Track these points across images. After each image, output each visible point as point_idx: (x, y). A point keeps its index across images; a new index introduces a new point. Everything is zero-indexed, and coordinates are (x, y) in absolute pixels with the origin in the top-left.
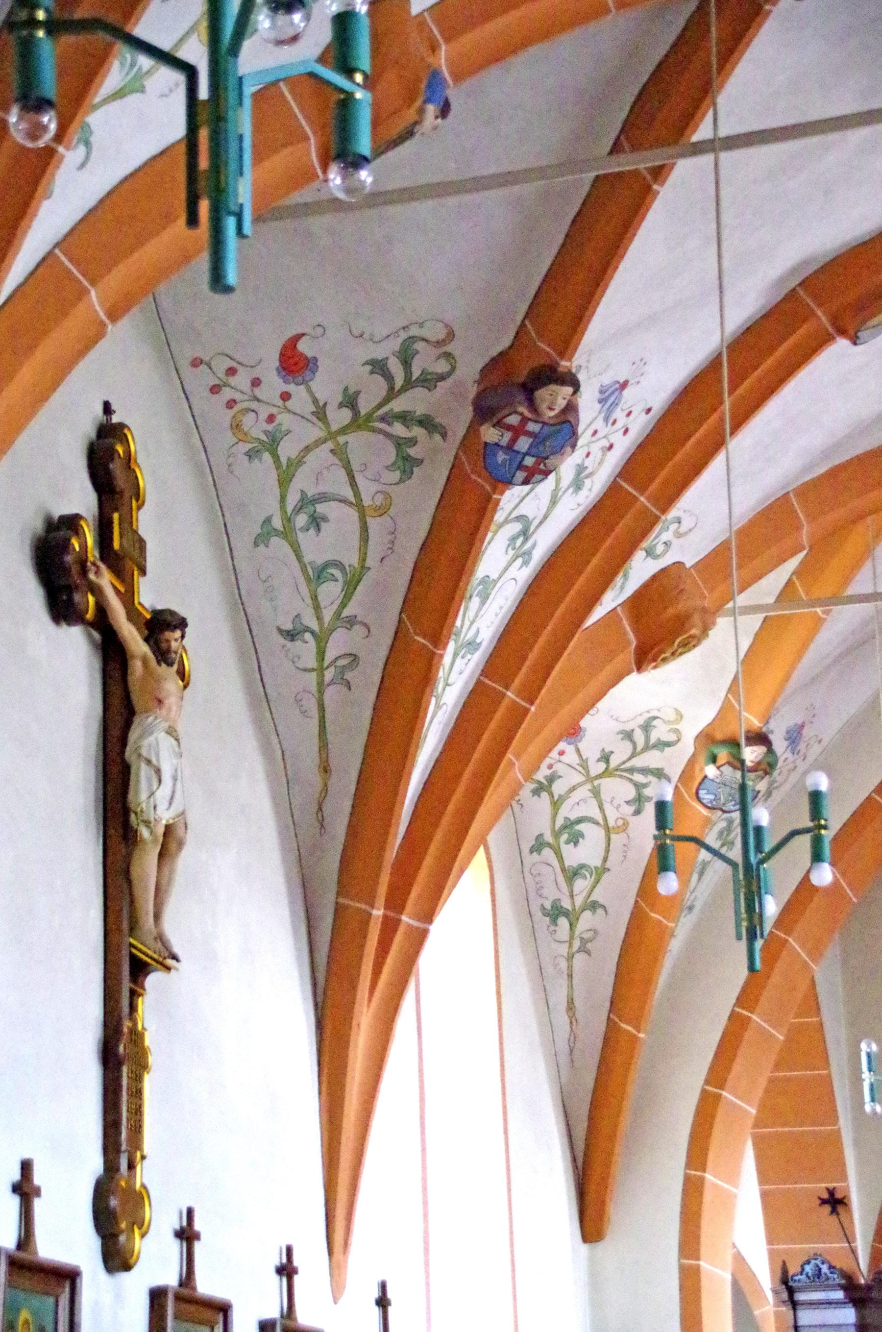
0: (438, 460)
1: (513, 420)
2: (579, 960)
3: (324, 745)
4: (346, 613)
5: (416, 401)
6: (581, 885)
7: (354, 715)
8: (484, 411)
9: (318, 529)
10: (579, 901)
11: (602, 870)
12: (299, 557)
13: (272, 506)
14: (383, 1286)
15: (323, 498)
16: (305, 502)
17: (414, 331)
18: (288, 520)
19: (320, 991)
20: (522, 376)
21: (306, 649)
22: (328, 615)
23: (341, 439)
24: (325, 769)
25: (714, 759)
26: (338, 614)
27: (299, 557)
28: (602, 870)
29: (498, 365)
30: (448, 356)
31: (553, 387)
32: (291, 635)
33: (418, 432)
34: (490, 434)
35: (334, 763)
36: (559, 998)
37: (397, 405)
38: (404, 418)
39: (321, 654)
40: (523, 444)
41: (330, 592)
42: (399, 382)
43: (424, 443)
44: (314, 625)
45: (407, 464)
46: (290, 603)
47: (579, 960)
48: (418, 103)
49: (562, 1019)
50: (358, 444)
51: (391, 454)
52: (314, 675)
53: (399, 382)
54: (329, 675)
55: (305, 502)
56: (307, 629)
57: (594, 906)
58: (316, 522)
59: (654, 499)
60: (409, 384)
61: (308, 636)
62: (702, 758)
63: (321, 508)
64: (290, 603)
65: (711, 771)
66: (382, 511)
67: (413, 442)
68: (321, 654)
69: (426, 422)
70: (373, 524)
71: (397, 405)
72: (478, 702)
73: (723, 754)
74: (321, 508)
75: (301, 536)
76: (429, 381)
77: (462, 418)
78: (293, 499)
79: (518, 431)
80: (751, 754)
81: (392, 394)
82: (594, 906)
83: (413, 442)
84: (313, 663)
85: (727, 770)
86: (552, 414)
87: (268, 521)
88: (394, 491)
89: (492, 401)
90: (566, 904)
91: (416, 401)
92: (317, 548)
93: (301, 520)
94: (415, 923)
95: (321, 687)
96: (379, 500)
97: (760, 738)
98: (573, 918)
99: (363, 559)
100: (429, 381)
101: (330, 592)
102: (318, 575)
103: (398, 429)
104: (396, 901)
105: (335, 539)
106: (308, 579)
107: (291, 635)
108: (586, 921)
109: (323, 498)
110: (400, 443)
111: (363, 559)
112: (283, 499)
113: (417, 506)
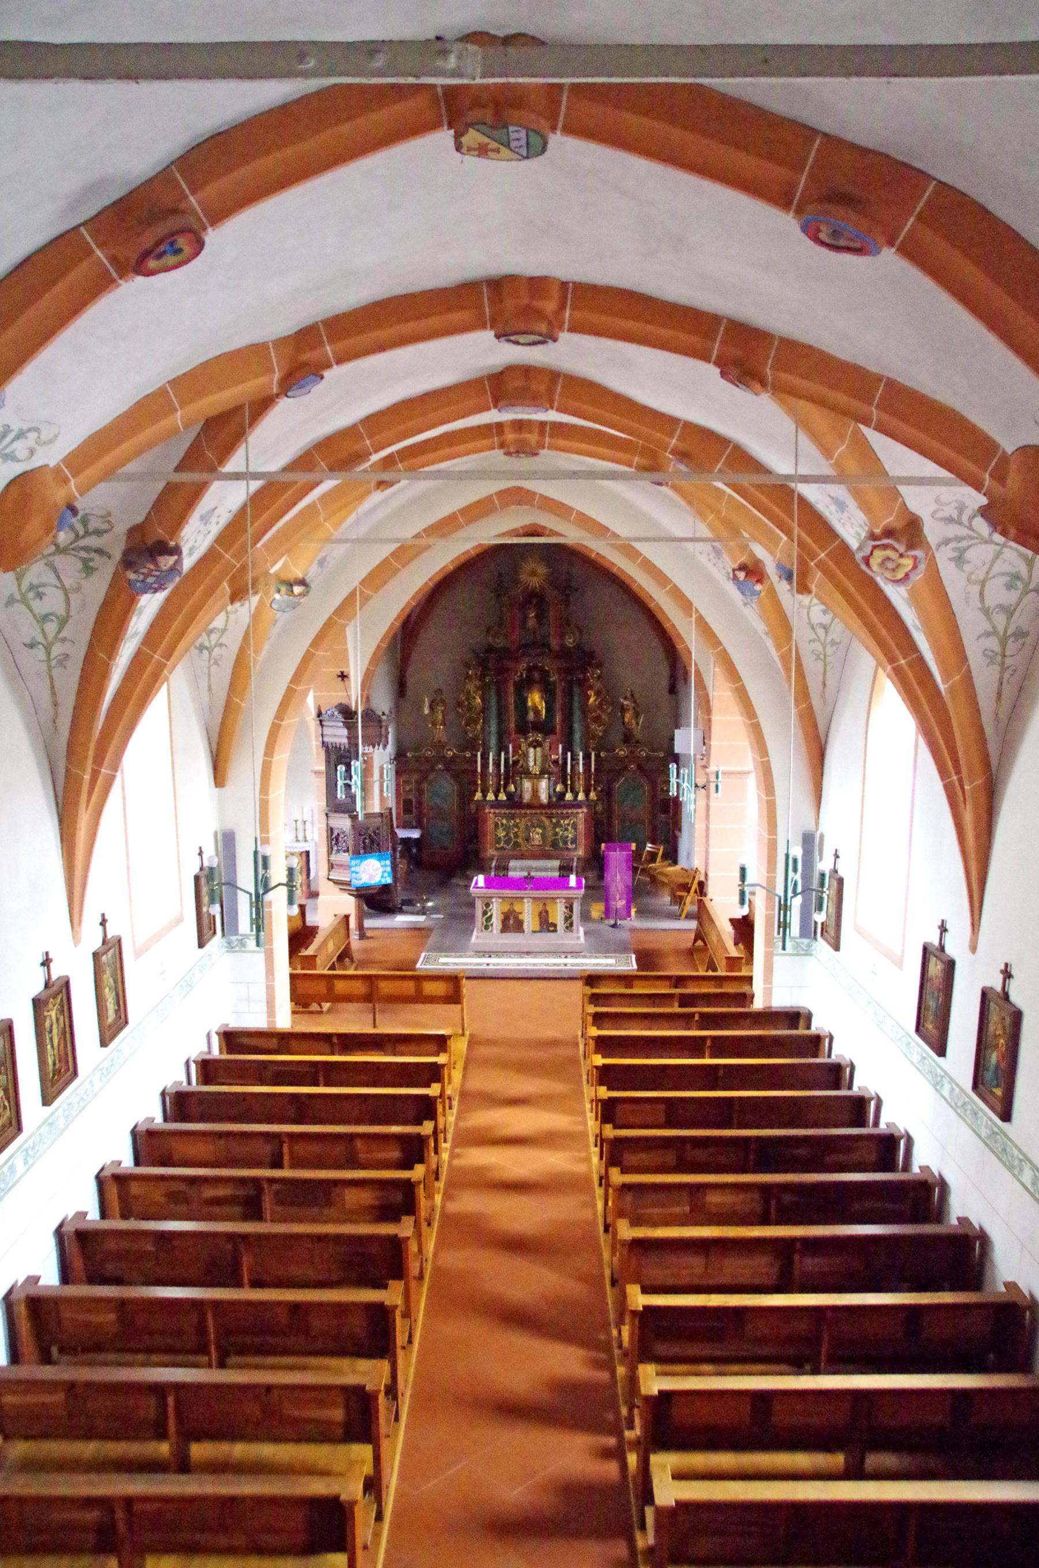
0: (106, 570)
1: (145, 571)
2: (214, 669)
3: (54, 693)
4: (61, 635)
5: (93, 541)
6: (214, 637)
7: (69, 680)
8: (128, 562)
9: (41, 599)
10: (213, 643)
11: (223, 631)
12: (31, 611)
13: (14, 589)
14: (103, 915)
15: (43, 585)
16: (32, 587)
17: (87, 511)
18: (24, 596)
19: (60, 806)
20: (150, 542)
21: (40, 653)
22: (50, 637)
23: (51, 559)
24: (55, 704)
25: (279, 591)
26: (56, 637)
27: (31, 611)
28: (223, 631)
29: (136, 531)
30: (109, 522)
31: (167, 557)
32: (31, 646)
33: (93, 555)
34: (132, 576)
35: (59, 700)
36: (204, 684)
37: (82, 543)
38: (85, 549)
39: (49, 654)
40: (150, 580)
41: (51, 627)
42: (81, 533)
43: (98, 561)
44: (43, 641)
45: (88, 569)
46: (29, 630)
47: (214, 669)
48: (54, 531)
49: (205, 695)
50: (59, 560)
51: (80, 565)
52: (45, 664)
53: (81, 533)
54: (53, 663)
55: (32, 587)
56: (39, 643)
57: (221, 645)
58: (40, 596)
59: (234, 556)
60: (87, 533)
61: (40, 646)
62: (273, 589)
63: (41, 590)
64: (29, 630)
65: (277, 596)
66: (78, 589)
67: (92, 560)
68: (49, 654)
69: (100, 551)
70: (73, 597)
71: (82, 543)
72: (139, 661)
73: (283, 589)
74: (41, 590)
75: (31, 602)
76: (98, 533)
77: (117, 554)
78: (25, 585)
79: (146, 576)
80: (297, 589)
81: (77, 537)
82: (221, 645)
83: (92, 560)
84: (45, 658)
85: (286, 597)
86: (165, 568)
87: (12, 595)
88: (83, 582)
89: (133, 557)
90: (207, 644)
91: (93, 541)
92: (40, 607)
93: (31, 595)
94: (109, 772)
95: (49, 668)
96: (75, 585)
97: (302, 582)
98: (210, 650)
99: (68, 611)
100: (98, 533)
101: (51, 627)
102: (45, 619)
103: (83, 554)
104: (99, 760)
105: (53, 602)
106: (38, 621)
107: (31, 646)
108: (217, 651)
109: (43, 585)
110: (85, 561)
111: (68, 611)
112: (19, 585)
113: (97, 588)
